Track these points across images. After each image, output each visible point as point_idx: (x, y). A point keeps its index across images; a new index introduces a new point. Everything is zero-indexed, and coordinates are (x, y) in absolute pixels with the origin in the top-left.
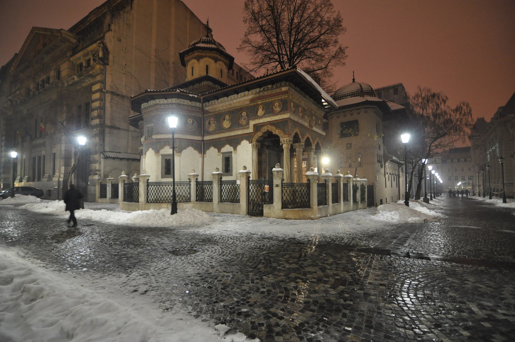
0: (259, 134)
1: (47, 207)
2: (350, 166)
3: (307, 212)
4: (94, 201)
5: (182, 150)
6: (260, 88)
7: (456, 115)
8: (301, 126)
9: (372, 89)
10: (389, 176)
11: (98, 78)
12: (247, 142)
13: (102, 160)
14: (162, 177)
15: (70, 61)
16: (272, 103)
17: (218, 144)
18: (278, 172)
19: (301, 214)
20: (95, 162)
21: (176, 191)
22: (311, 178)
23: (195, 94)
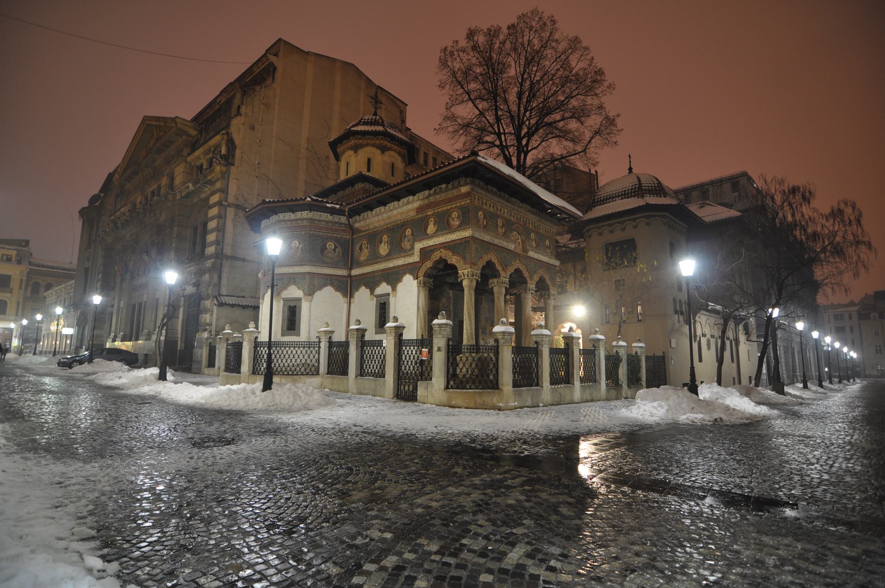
0: (429, 264)
3: (492, 398)
4: (199, 372)
5: (314, 292)
6: (430, 189)
7: (834, 225)
9: (659, 183)
10: (708, 341)
11: (218, 185)
13: (215, 307)
14: (283, 335)
15: (186, 162)
16: (448, 214)
17: (371, 282)
18: (440, 325)
19: (479, 400)
21: (273, 356)
22: (500, 337)
23: (337, 204)
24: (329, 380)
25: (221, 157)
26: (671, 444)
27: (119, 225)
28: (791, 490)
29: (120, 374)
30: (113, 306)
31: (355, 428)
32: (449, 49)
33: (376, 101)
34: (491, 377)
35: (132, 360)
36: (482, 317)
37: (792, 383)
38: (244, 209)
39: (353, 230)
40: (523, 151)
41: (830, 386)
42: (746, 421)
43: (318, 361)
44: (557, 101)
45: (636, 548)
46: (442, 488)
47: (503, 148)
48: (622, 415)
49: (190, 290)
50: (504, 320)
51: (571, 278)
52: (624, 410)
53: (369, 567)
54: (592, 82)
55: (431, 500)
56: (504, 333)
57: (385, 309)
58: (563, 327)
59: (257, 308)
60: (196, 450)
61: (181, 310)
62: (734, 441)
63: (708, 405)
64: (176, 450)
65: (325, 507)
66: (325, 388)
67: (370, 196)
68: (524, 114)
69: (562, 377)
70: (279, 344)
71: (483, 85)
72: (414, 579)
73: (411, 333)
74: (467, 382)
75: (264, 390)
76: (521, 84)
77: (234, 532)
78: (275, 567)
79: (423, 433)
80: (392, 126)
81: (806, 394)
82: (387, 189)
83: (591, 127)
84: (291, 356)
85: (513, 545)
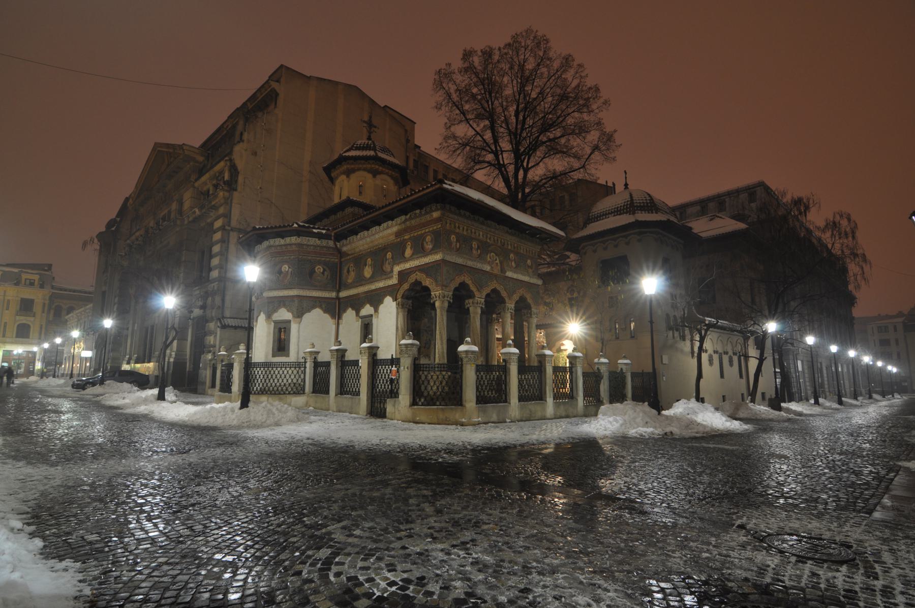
0: (406, 286)
1: (124, 398)
2: (617, 338)
3: (456, 415)
4: (203, 393)
9: (652, 199)
11: (221, 210)
14: (273, 356)
16: (422, 238)
18: (406, 345)
19: (441, 416)
20: (211, 333)
25: (224, 183)
33: (370, 125)
35: (142, 382)
54: (582, 98)
56: (467, 352)
59: (250, 330)
73: (387, 351)
80: (385, 150)
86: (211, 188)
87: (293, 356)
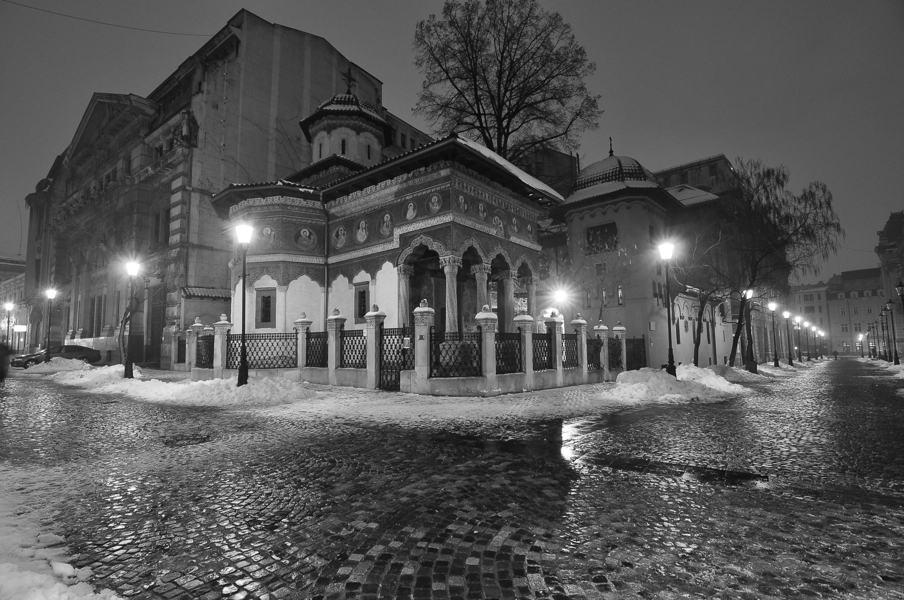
0: (409, 251)
3: (476, 385)
4: (168, 368)
6: (409, 173)
7: (805, 207)
8: (480, 234)
9: (640, 166)
10: (686, 323)
11: (180, 169)
12: (391, 265)
15: (144, 143)
16: (427, 198)
18: (422, 313)
19: (462, 387)
20: (173, 304)
21: (248, 350)
23: (310, 188)
24: (308, 373)
25: (182, 138)
26: (650, 424)
27: (72, 212)
28: (762, 463)
29: (82, 372)
30: (69, 301)
31: (336, 420)
32: (426, 23)
34: (475, 364)
35: (93, 358)
36: (465, 304)
37: (764, 362)
38: (210, 194)
39: (328, 216)
40: (503, 133)
41: (799, 363)
42: (721, 400)
43: (296, 353)
44: (538, 81)
45: (616, 524)
46: (427, 476)
47: (483, 129)
48: (604, 398)
49: (154, 281)
50: (487, 306)
51: (553, 265)
52: (605, 393)
53: (354, 557)
54: (573, 61)
55: (416, 488)
56: (486, 319)
57: (364, 297)
58: (546, 313)
59: (228, 299)
60: (169, 449)
61: (146, 302)
62: (709, 419)
63: (685, 385)
64: (147, 450)
65: (308, 500)
66: (304, 380)
67: (345, 180)
68: (505, 94)
69: (545, 363)
70: (253, 337)
71: (462, 62)
72: (401, 566)
73: (392, 322)
74: (451, 370)
75: (239, 385)
76: (501, 63)
77: (213, 530)
78: (257, 563)
79: (406, 422)
80: (367, 105)
81: (777, 372)
82: (363, 172)
83: (573, 108)
84: (267, 348)
85: (498, 528)
86: (165, 145)
87: (280, 327)
